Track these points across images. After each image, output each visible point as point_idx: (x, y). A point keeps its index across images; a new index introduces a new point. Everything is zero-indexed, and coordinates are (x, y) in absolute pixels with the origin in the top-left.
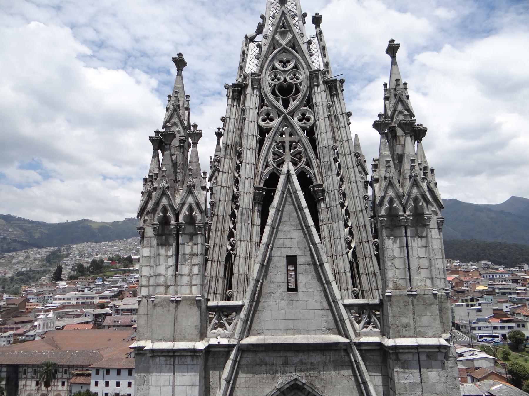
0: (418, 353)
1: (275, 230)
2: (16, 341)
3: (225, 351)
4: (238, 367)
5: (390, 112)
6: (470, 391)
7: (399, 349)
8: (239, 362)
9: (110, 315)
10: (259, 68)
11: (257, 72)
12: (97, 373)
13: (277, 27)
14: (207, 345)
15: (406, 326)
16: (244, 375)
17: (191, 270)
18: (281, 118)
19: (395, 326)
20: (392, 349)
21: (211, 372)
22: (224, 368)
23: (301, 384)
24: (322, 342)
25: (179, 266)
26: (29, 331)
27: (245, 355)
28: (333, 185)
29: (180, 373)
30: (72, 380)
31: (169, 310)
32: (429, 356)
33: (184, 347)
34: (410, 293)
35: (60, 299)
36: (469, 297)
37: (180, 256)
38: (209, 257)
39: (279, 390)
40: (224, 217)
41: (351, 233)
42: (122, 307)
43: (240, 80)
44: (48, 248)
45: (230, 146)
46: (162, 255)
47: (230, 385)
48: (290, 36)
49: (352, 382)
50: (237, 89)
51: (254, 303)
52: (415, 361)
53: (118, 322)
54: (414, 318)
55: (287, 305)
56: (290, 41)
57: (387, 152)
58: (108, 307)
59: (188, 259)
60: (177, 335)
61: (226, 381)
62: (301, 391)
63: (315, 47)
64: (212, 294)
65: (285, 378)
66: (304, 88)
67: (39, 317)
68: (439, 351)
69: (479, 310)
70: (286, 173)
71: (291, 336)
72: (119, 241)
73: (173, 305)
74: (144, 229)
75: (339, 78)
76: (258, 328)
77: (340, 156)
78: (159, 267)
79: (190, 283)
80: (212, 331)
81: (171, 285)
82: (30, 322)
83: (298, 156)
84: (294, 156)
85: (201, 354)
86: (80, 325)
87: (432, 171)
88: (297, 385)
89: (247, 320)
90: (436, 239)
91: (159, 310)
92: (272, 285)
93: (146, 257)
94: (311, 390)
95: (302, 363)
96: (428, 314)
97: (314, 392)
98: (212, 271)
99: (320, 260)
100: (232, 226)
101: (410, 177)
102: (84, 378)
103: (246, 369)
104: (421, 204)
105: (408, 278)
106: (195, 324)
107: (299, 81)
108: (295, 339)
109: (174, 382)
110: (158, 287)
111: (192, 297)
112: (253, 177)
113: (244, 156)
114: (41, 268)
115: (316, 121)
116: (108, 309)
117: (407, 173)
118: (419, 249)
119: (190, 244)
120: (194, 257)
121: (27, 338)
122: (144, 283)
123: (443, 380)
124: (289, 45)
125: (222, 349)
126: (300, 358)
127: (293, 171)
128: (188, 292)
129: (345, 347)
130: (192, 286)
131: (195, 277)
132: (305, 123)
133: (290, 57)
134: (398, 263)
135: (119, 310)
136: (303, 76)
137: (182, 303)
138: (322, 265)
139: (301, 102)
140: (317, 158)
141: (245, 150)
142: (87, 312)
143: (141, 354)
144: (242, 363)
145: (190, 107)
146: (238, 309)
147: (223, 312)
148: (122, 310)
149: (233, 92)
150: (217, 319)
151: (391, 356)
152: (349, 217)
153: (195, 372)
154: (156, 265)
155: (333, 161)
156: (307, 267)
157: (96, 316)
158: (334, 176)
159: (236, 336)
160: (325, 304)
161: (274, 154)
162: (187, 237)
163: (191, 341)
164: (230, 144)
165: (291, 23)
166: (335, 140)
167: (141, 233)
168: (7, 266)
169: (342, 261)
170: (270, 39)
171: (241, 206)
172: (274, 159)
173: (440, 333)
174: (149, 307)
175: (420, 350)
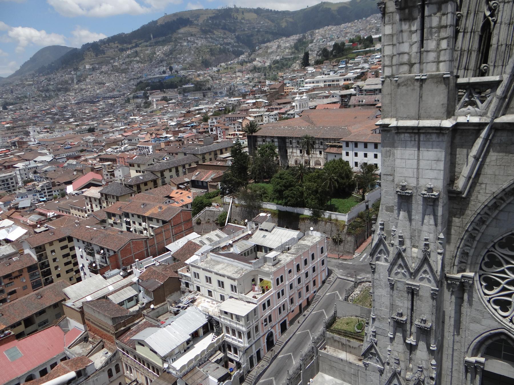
2: (281, 119)
3: (474, 129)
4: (489, 146)
8: (491, 140)
9: (355, 95)
12: (347, 145)
14: (454, 123)
16: (496, 154)
17: (438, 45)
21: (458, 149)
22: (472, 146)
25: (425, 42)
26: (290, 110)
27: (499, 134)
29: (425, 149)
30: (328, 150)
33: (429, 125)
35: (310, 83)
37: (425, 30)
38: (461, 28)
42: (366, 87)
44: (295, 36)
46: (406, 31)
47: (479, 163)
53: (362, 101)
58: (352, 88)
59: (435, 33)
61: (475, 157)
64: (463, 71)
67: (296, 99)
72: (358, 21)
73: (417, 84)
74: (385, 4)
78: (402, 44)
79: (436, 60)
80: (462, 109)
81: (415, 63)
82: (289, 103)
85: (447, 132)
86: (329, 105)
89: (505, 97)
91: (403, 89)
93: (388, 35)
98: (464, 44)
102: (337, 149)
103: (498, 147)
106: (442, 103)
109: (418, 156)
110: (402, 66)
111: (439, 74)
114: (291, 55)
116: (353, 90)
119: (438, 14)
120: (442, 30)
121: (289, 116)
122: (387, 62)
128: (434, 69)
130: (439, 62)
131: (442, 52)
135: (363, 90)
137: (428, 81)
142: (334, 93)
143: (386, 130)
144: (495, 141)
146: (494, 85)
147: (474, 89)
148: (366, 90)
150: (468, 97)
153: (441, 148)
154: (399, 43)
157: (342, 96)
159: (489, 114)
162: (434, 8)
167: (382, 9)
168: (264, 56)
174: (393, 87)
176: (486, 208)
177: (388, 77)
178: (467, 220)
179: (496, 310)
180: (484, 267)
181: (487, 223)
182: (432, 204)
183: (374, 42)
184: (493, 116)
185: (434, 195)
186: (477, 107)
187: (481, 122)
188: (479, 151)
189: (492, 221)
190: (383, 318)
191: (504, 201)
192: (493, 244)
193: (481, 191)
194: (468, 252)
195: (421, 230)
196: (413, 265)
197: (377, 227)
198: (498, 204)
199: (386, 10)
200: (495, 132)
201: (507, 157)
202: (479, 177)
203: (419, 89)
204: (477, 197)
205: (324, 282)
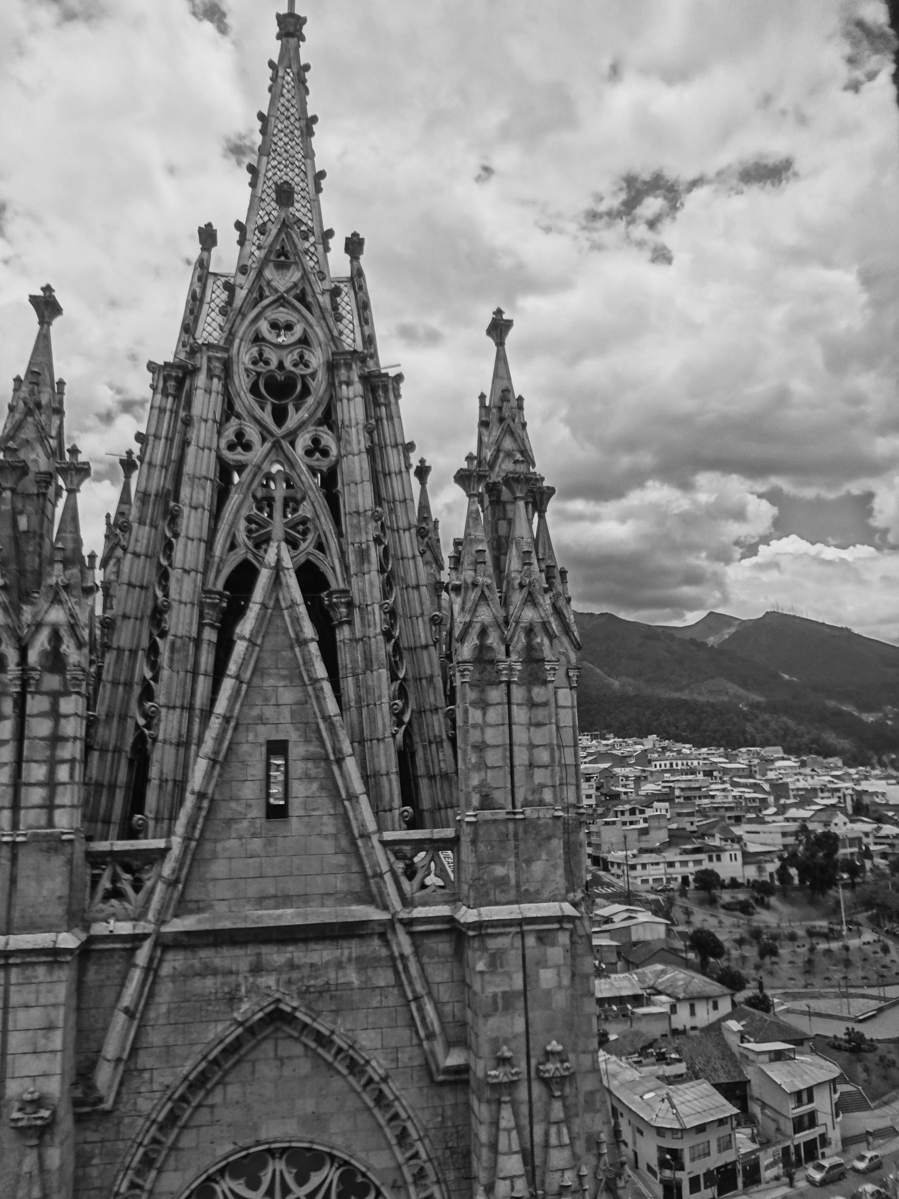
1: (244, 686)
5: (489, 454)
6: (620, 988)
7: (487, 927)
10: (225, 335)
11: (221, 343)
13: (270, 252)
15: (502, 882)
17: (52, 772)
18: (268, 445)
20: (474, 930)
23: (288, 1009)
24: (334, 921)
27: (170, 956)
28: (371, 592)
32: (543, 938)
33: (30, 946)
34: (512, 816)
36: (627, 807)
39: (241, 1024)
40: (133, 653)
41: (402, 693)
43: (182, 356)
45: (153, 497)
47: (136, 1023)
48: (294, 275)
49: (393, 998)
50: (174, 374)
51: (193, 844)
52: (517, 948)
55: (265, 846)
56: (295, 285)
57: (480, 534)
63: (347, 303)
65: (255, 999)
66: (319, 385)
69: (644, 832)
70: (273, 565)
75: (392, 373)
76: (202, 896)
77: (388, 532)
83: (301, 528)
84: (293, 528)
85: (69, 958)
87: (563, 573)
88: (281, 1011)
92: (233, 805)
96: (544, 857)
97: (315, 1025)
99: (337, 750)
100: (148, 675)
101: (521, 586)
103: (170, 985)
104: (538, 640)
105: (509, 786)
106: (58, 894)
107: (309, 371)
108: (280, 917)
111: (52, 834)
112: (201, 569)
113: (183, 522)
115: (340, 457)
117: (515, 578)
118: (532, 729)
123: (566, 982)
124: (292, 293)
126: (288, 955)
127: (287, 562)
128: (43, 821)
129: (379, 929)
132: (318, 460)
133: (293, 317)
134: (493, 757)
136: (317, 359)
138: (340, 761)
139: (311, 416)
140: (340, 534)
141: (186, 510)
145: (65, 408)
149: (165, 381)
152: (401, 659)
155: (372, 544)
156: (310, 765)
158: (374, 574)
159: (151, 916)
160: (344, 843)
161: (249, 520)
163: (49, 928)
164: (153, 492)
165: (299, 247)
166: (378, 499)
169: (382, 751)
170: (253, 274)
171: (172, 632)
172: (249, 531)
173: (563, 892)
175: (526, 928)
176: (154, 1127)
178: (118, 1166)
181: (158, 1165)
182: (34, 1142)
184: (157, 920)
185: (42, 1118)
186: (130, 903)
187: (137, 932)
188: (135, 996)
189: (167, 1155)
191: (188, 1102)
198: (178, 1112)
200: (163, 952)
201: (186, 1004)
202: (136, 1056)
204: (135, 1103)
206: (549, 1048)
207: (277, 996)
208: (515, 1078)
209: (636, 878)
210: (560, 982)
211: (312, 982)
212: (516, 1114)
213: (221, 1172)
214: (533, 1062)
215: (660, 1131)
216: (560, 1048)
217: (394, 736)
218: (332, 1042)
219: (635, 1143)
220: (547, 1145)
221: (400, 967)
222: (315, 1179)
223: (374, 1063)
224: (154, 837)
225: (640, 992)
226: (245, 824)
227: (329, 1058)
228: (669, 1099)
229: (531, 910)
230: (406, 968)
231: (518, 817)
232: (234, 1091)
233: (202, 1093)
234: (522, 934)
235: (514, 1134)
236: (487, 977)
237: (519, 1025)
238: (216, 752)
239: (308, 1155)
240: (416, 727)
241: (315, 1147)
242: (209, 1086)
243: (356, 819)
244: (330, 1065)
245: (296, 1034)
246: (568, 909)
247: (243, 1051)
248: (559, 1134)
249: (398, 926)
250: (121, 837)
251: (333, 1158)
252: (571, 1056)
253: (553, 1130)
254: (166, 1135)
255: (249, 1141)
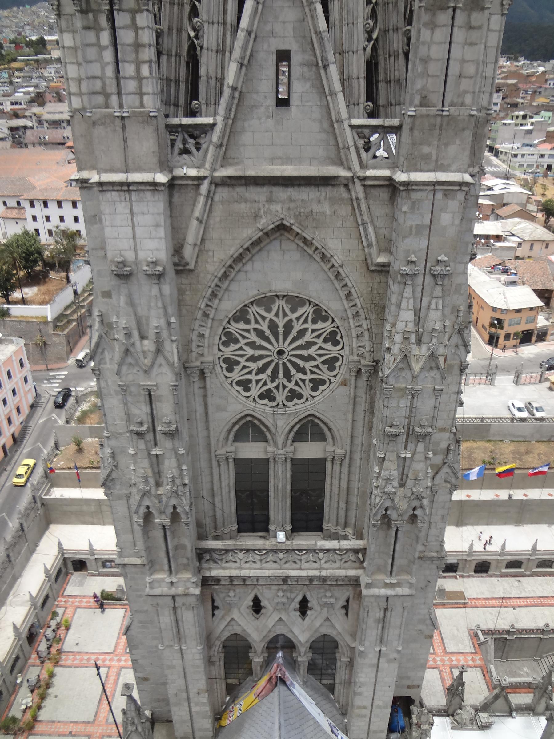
0: (434, 191)
1: (260, 6)
3: (194, 185)
7: (412, 185)
15: (426, 158)
17: (138, 70)
19: (413, 157)
23: (288, 224)
25: (120, 64)
27: (220, 189)
31: (115, 131)
32: (446, 194)
34: (440, 113)
36: (522, 113)
39: (262, 230)
41: (374, 15)
42: (46, 116)
47: (203, 226)
49: (350, 222)
51: (230, 122)
54: (438, 147)
60: (131, 165)
62: (289, 232)
68: (460, 190)
69: (529, 132)
71: (279, 167)
73: (118, 122)
79: (139, 91)
89: (221, 145)
90: (494, 31)
92: (255, 96)
93: (69, 48)
94: (299, 231)
95: (291, 200)
97: (303, 234)
103: (221, 206)
105: (442, 90)
108: (284, 170)
111: (144, 112)
118: (466, 47)
122: (74, 89)
123: (457, 222)
125: (190, 182)
126: (289, 194)
128: (137, 103)
129: (345, 182)
138: (325, 67)
144: (217, 198)
148: (47, 121)
151: (401, 193)
156: (306, 69)
159: (207, 165)
160: (326, 125)
163: (150, 170)
167: (55, 7)
173: (466, 166)
175: (437, 187)
177: (78, 110)
179: (238, 392)
180: (222, 348)
182: (156, 281)
183: (49, 48)
184: (211, 168)
189: (224, 293)
190: (120, 434)
192: (227, 319)
193: (209, 260)
194: (204, 333)
195: (148, 317)
196: (146, 361)
197: (94, 320)
198: (228, 273)
199: (61, 9)
200: (216, 187)
203: (121, 130)
205: (32, 406)
206: (439, 258)
207: (282, 216)
208: (417, 272)
209: (515, 163)
210: (453, 222)
211: (302, 210)
212: (414, 291)
213: (252, 303)
214: (428, 265)
215: (494, 309)
216: (446, 259)
217: (364, 49)
218: (312, 244)
219: (478, 313)
220: (429, 308)
221: (356, 205)
222: (300, 311)
223: (335, 257)
224: (206, 116)
225: (500, 233)
226: (262, 109)
227: (311, 252)
228: (504, 293)
229: (443, 176)
230: (359, 205)
231: (445, 113)
232: (257, 265)
233: (241, 264)
234: (434, 191)
235: (411, 301)
236: (408, 215)
237: (424, 244)
238: (243, 58)
239: (297, 299)
240: (380, 42)
241: (301, 296)
242: (244, 261)
243: (334, 109)
244: (311, 256)
245: (292, 238)
246: (467, 178)
247: (262, 245)
248: (437, 303)
249: (356, 180)
250: (186, 116)
251: (310, 302)
252: (452, 264)
253: (434, 301)
254: (223, 284)
255: (266, 290)
